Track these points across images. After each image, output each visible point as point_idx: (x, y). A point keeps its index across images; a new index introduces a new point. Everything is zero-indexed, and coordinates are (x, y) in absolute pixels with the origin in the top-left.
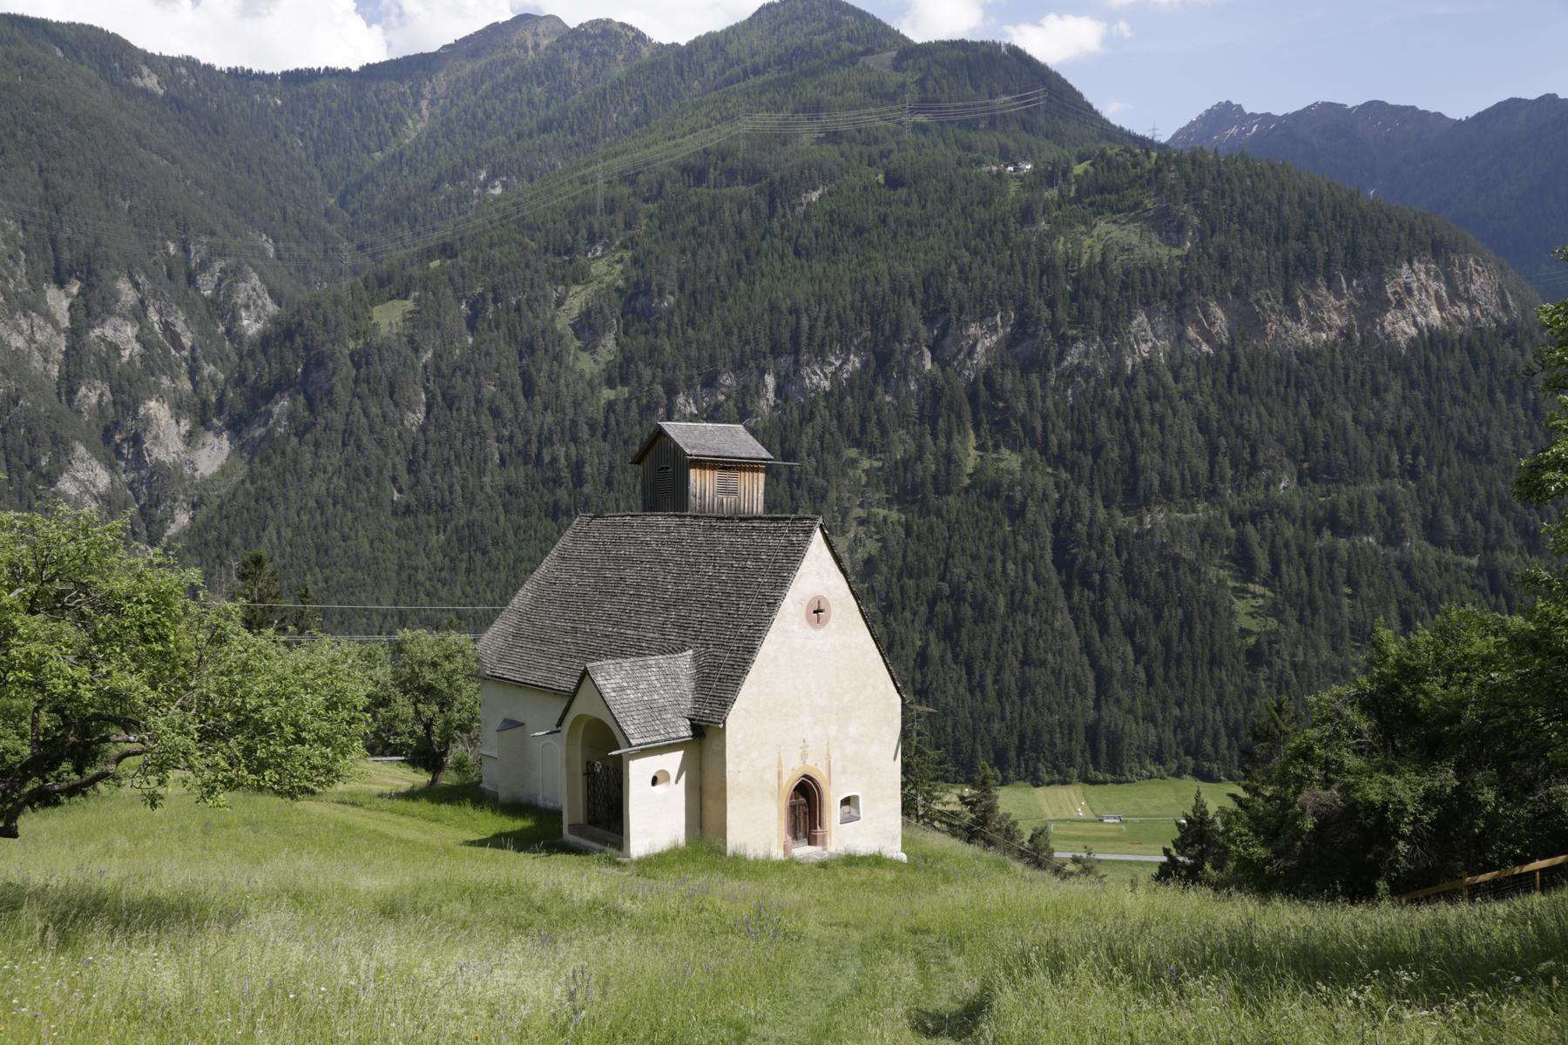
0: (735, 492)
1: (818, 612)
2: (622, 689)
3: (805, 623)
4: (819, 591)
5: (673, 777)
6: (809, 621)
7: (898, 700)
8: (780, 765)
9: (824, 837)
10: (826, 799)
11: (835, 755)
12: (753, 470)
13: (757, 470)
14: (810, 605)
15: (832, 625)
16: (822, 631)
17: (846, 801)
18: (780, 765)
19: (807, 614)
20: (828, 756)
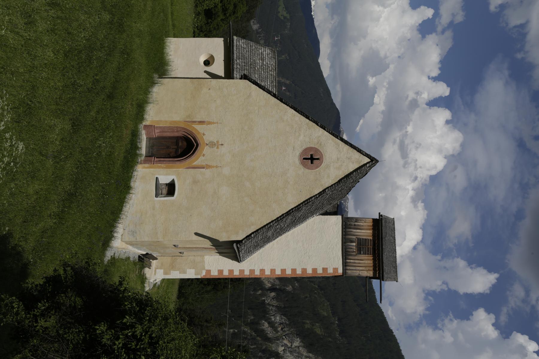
1: (311, 158)
2: (263, 60)
3: (304, 147)
4: (326, 160)
5: (208, 69)
7: (240, 239)
8: (209, 123)
9: (151, 161)
10: (178, 163)
11: (207, 172)
13: (375, 270)
14: (316, 150)
15: (302, 170)
16: (297, 161)
17: (171, 189)
18: (209, 123)
19: (310, 149)
20: (208, 167)
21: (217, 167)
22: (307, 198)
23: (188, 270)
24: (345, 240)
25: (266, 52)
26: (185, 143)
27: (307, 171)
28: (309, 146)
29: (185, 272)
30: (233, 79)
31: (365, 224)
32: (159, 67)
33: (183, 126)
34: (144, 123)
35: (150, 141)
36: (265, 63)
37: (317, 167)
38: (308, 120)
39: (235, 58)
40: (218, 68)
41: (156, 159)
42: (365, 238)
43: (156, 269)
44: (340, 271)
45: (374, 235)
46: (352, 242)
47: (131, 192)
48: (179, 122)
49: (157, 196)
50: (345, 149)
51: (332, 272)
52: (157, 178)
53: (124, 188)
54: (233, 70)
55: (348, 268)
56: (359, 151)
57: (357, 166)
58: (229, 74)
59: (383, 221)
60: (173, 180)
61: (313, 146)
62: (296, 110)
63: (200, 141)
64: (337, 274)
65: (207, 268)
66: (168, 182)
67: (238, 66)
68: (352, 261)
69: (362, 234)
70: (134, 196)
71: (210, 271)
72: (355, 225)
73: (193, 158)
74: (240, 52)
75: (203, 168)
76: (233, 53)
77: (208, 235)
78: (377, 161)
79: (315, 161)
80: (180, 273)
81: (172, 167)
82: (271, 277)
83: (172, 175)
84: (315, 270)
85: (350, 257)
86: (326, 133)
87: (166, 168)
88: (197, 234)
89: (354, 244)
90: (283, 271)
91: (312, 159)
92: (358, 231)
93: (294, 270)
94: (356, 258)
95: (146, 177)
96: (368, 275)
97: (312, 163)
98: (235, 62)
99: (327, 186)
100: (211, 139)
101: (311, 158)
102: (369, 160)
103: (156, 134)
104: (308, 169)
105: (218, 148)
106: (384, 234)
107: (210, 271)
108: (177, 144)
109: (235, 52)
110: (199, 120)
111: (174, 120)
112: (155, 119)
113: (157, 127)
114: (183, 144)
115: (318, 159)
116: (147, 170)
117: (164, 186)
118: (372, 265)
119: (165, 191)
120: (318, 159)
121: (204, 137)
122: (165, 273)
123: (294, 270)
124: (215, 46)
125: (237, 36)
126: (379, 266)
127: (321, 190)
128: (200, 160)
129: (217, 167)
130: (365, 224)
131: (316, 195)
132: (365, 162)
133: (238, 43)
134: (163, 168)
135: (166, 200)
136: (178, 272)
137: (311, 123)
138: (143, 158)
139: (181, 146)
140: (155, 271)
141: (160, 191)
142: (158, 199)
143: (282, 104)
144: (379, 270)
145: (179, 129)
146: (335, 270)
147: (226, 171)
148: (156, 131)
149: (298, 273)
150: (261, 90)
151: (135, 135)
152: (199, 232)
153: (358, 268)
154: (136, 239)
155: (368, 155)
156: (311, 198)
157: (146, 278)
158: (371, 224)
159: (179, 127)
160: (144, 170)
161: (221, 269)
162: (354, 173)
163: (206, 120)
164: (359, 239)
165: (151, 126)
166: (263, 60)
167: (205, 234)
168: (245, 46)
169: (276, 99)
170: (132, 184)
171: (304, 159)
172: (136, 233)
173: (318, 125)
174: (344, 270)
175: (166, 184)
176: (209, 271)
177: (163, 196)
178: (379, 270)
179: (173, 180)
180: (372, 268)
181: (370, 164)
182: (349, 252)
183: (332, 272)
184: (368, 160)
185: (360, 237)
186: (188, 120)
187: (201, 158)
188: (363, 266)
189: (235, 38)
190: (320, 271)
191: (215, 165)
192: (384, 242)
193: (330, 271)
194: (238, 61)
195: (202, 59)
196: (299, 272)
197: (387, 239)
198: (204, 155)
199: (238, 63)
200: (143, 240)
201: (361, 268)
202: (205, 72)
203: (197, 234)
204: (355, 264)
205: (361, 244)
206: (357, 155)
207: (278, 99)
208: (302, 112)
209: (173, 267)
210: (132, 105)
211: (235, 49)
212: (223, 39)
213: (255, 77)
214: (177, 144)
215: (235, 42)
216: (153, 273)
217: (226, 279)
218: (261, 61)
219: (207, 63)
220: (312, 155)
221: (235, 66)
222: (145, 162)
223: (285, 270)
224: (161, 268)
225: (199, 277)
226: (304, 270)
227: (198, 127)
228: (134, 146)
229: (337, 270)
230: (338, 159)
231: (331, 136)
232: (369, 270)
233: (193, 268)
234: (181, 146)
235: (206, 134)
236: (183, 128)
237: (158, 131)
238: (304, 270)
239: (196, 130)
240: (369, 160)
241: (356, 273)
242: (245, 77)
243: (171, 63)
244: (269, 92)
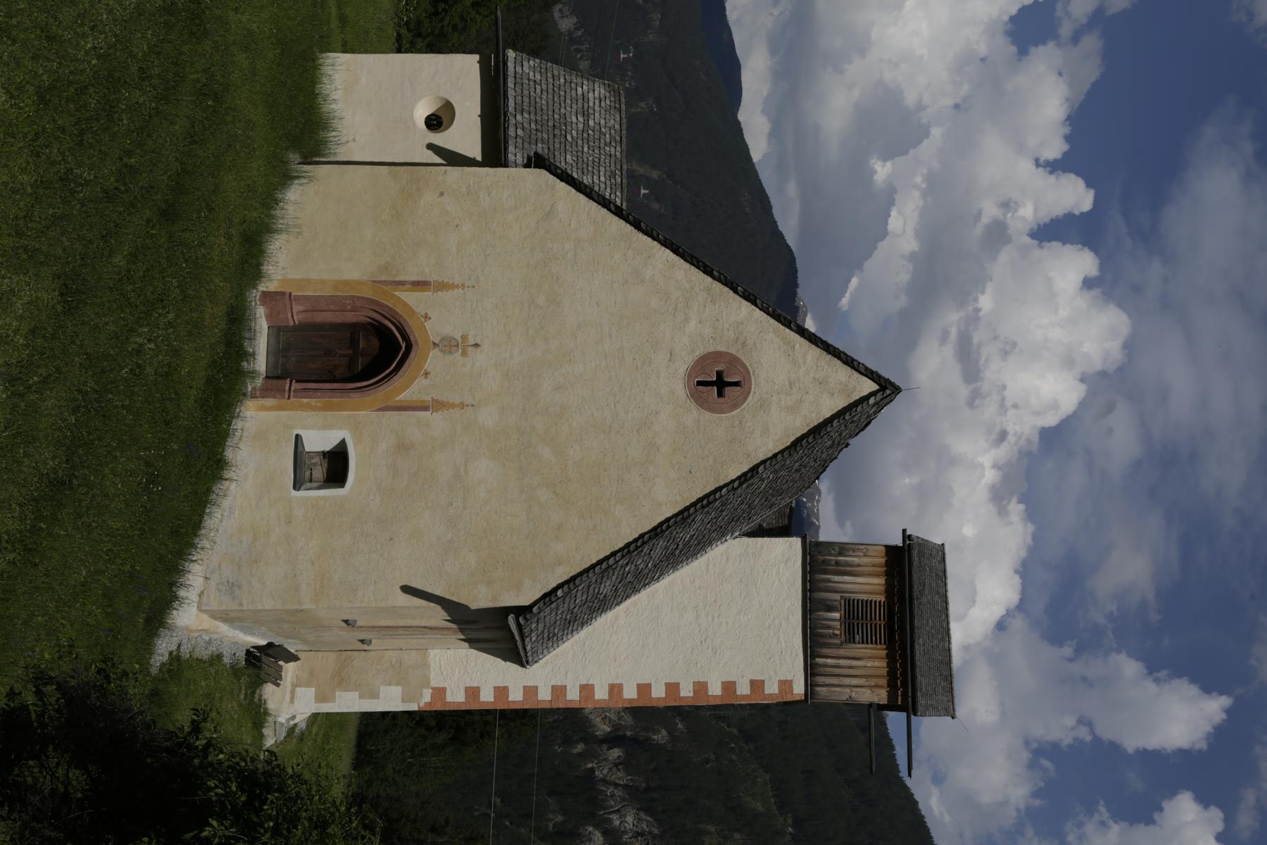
0: (850, 635)
1: (719, 382)
2: (586, 115)
3: (699, 353)
5: (439, 139)
6: (704, 361)
7: (525, 600)
8: (442, 286)
10: (356, 398)
11: (437, 421)
12: (892, 676)
13: (892, 685)
14: (733, 360)
15: (694, 415)
16: (681, 390)
17: (336, 466)
18: (442, 286)
19: (716, 356)
20: (436, 406)
21: (462, 406)
22: (707, 490)
23: (382, 688)
24: (812, 604)
25: (596, 92)
26: (375, 342)
27: (708, 415)
28: (711, 349)
29: (374, 695)
30: (506, 166)
31: (865, 560)
32: (303, 133)
33: (367, 293)
34: (262, 287)
35: (278, 336)
36: (591, 123)
37: (735, 406)
38: (710, 279)
39: (511, 109)
40: (466, 135)
41: (295, 385)
42: (865, 597)
43: (294, 686)
44: (799, 689)
45: (889, 590)
46: (830, 609)
47: (227, 474)
48: (359, 283)
49: (297, 486)
50: (809, 358)
51: (776, 691)
52: (297, 436)
53: (207, 465)
54: (506, 143)
55: (820, 680)
56: (849, 362)
57: (841, 403)
58: (494, 154)
59: (915, 553)
60: (343, 444)
61: (724, 349)
62: (676, 251)
63: (415, 336)
64: (789, 698)
65: (434, 684)
66: (327, 449)
67: (520, 132)
68: (829, 661)
69: (857, 587)
70: (233, 486)
71: (444, 690)
72: (837, 563)
73: (397, 381)
74: (526, 92)
75: (426, 409)
76: (506, 96)
77: (438, 592)
78: (897, 390)
79: (728, 391)
80: (361, 697)
81: (339, 408)
82: (611, 705)
83: (341, 428)
84: (729, 687)
85: (825, 651)
86: (758, 313)
87: (327, 408)
88: (407, 589)
89: (837, 615)
90: (644, 689)
91: (721, 384)
92: (846, 578)
93: (672, 688)
94: (842, 652)
95: (267, 434)
96: (876, 700)
97: (720, 394)
98: (512, 121)
99: (762, 457)
100: (448, 330)
101: (719, 382)
102: (875, 387)
103: (296, 315)
104: (712, 410)
105: (464, 354)
106: (916, 588)
107: (444, 690)
108: (353, 342)
109: (511, 93)
110: (414, 278)
111: (346, 277)
112: (290, 276)
113: (298, 298)
114: (369, 345)
115: (736, 384)
116: (273, 414)
117: (316, 460)
118: (884, 671)
119: (319, 473)
120: (736, 384)
121: (428, 325)
122: (321, 698)
123: (672, 688)
124: (458, 77)
125: (515, 50)
126: (904, 675)
127: (745, 469)
128: (414, 387)
129: (462, 406)
130: (865, 560)
131: (733, 481)
132: (865, 393)
133: (519, 69)
134: (314, 409)
135: (324, 498)
136: (356, 694)
137: (718, 286)
138: (259, 382)
139: (363, 350)
140: (293, 693)
141: (308, 473)
142: (302, 493)
143: (640, 235)
144: (904, 685)
145: (358, 304)
146: (786, 685)
147: (487, 417)
148: (296, 308)
149: (683, 694)
150: (582, 196)
151: (237, 319)
152: (413, 585)
153: (847, 681)
154: (241, 604)
155: (872, 372)
156: (719, 489)
157: (266, 713)
158: (883, 560)
159: (359, 298)
160: (263, 414)
161: (475, 685)
162: (835, 423)
163: (433, 278)
164: (849, 602)
165: (283, 294)
166: (586, 115)
167: (430, 590)
168: (538, 77)
169: (622, 223)
170: (229, 454)
171: (699, 383)
172: (240, 587)
173: (736, 292)
174: (810, 685)
175: (324, 454)
176: (440, 692)
177: (315, 485)
178: (904, 685)
179: (343, 444)
180: (884, 682)
181: (879, 396)
182: (822, 636)
183: (776, 691)
184: (869, 386)
185: (853, 596)
186: (383, 278)
187: (421, 382)
188: (861, 675)
189: (511, 54)
190: (743, 689)
191: (458, 401)
192: (916, 611)
193: (772, 689)
194: (519, 117)
195: (422, 111)
196: (686, 692)
197: (924, 600)
198: (426, 374)
199: (518, 123)
200: (260, 607)
201: (855, 681)
202: (431, 147)
203: (407, 589)
204: (837, 671)
205: (855, 613)
206: (842, 373)
207: (627, 221)
208: (692, 257)
209: (341, 681)
210: (229, 237)
211: (510, 84)
212: (477, 57)
213: (566, 161)
214: (353, 342)
215: (510, 65)
216: (288, 697)
217: (488, 712)
218: (581, 119)
219: (434, 123)
220: (719, 374)
221: (511, 132)
222: (265, 392)
223: (649, 686)
224: (308, 685)
225: (414, 707)
226: (701, 687)
227: (411, 298)
228: (234, 348)
229: (791, 687)
230: (791, 384)
231: (772, 321)
232: (877, 686)
233: (398, 684)
234: (363, 350)
235: (433, 317)
236: (370, 300)
237: (301, 308)
238: (701, 687)
239: (405, 305)
240: (875, 387)
241: (843, 695)
242: (537, 162)
243: (335, 123)
244: (604, 203)
